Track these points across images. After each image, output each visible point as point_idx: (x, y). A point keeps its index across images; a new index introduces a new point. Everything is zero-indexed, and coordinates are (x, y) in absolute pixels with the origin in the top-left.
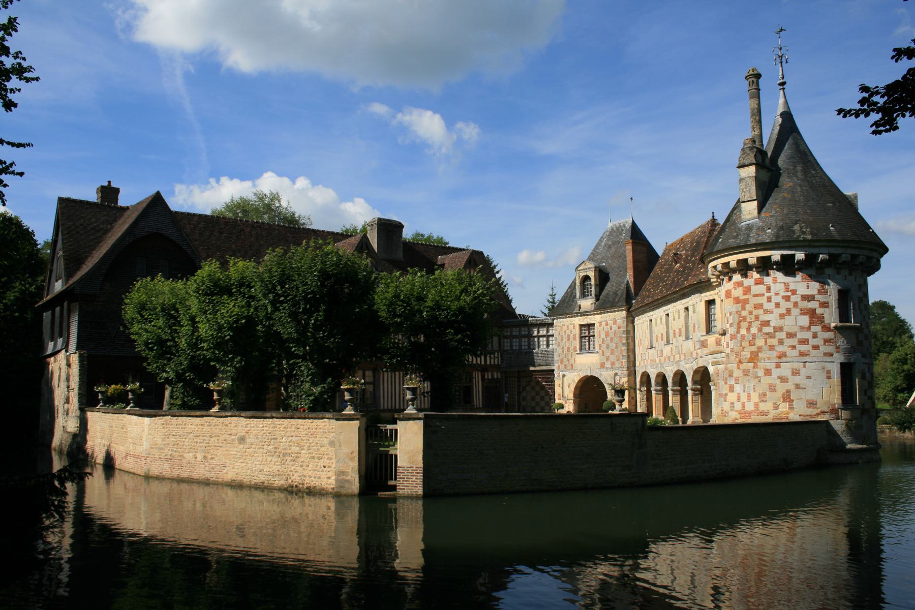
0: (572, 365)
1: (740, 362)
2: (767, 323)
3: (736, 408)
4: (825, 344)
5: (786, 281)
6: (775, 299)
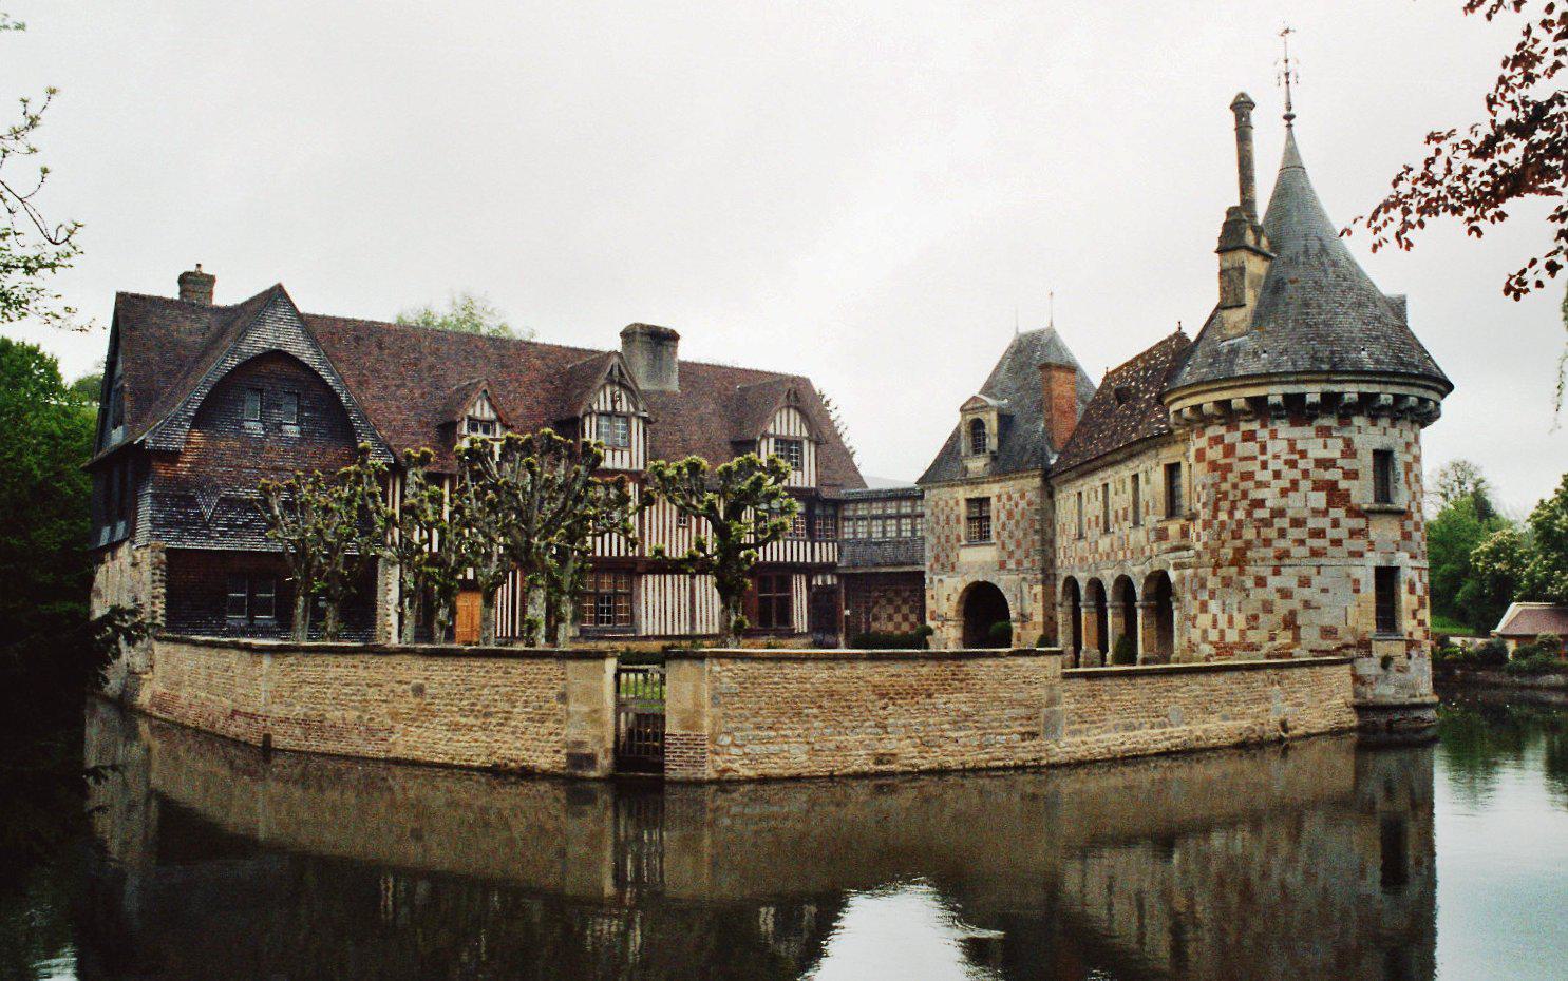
1: (1218, 565)
2: (1260, 503)
3: (1210, 639)
4: (1351, 537)
5: (1291, 436)
6: (1273, 466)
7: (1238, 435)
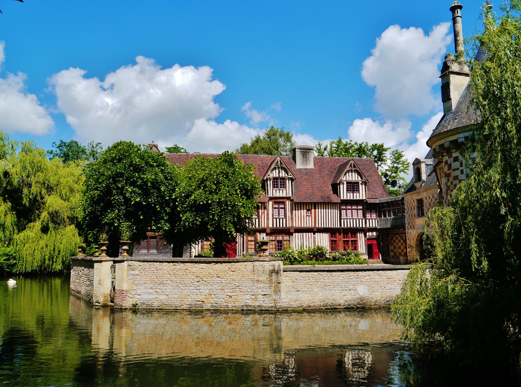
7: (452, 159)
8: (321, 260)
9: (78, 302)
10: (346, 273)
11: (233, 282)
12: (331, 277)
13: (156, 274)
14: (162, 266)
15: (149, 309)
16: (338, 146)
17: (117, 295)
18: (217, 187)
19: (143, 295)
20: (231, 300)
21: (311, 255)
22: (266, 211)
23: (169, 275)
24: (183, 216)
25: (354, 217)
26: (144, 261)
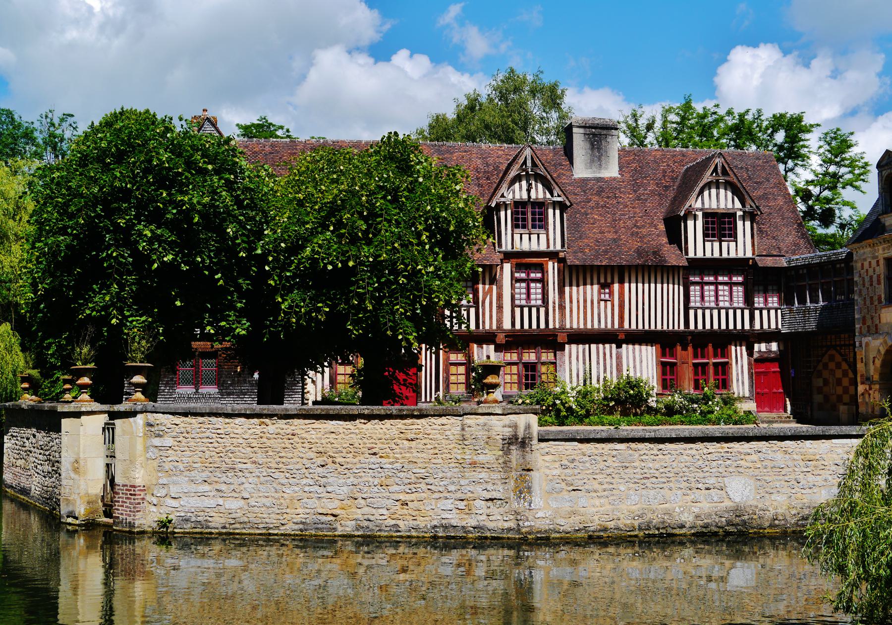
0: (876, 325)
8: (636, 415)
9: (23, 515)
10: (699, 445)
11: (411, 466)
12: (661, 456)
13: (216, 445)
14: (232, 425)
15: (201, 533)
16: (683, 118)
17: (121, 497)
18: (369, 226)
19: (186, 499)
20: (406, 512)
21: (611, 399)
22: (494, 287)
23: (249, 449)
24: (284, 300)
25: (721, 304)
26: (185, 414)
